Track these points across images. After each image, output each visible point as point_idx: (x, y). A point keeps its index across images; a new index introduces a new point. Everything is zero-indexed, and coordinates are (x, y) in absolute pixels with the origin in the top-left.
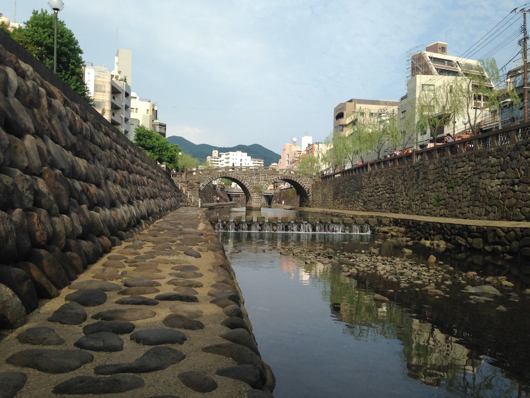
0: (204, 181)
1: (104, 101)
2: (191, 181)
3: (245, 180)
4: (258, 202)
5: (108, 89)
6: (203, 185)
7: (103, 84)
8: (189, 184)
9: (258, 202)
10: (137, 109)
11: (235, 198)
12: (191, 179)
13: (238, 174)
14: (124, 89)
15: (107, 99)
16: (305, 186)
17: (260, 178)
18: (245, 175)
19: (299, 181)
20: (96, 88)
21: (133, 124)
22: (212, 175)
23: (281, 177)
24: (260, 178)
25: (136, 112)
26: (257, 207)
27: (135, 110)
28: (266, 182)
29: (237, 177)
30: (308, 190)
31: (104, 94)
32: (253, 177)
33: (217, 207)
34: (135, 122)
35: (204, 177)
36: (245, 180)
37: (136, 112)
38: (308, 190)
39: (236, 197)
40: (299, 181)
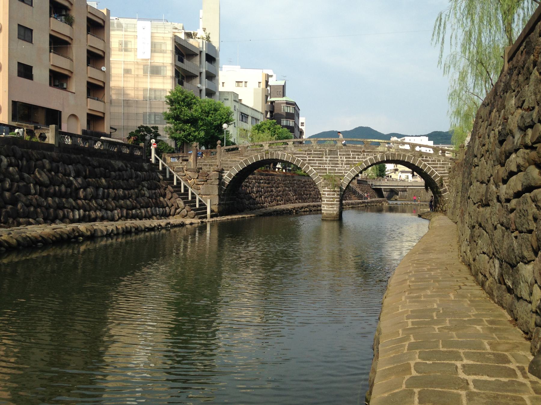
0: (231, 167)
1: (165, 65)
2: (205, 169)
3: (309, 163)
4: (332, 204)
5: (169, 47)
6: (230, 175)
7: (163, 41)
8: (202, 173)
9: (332, 204)
10: (246, 82)
11: (401, 193)
12: (206, 165)
13: (295, 154)
14: (204, 49)
15: (168, 62)
17: (339, 159)
18: (308, 154)
19: (420, 163)
20: (155, 48)
21: (228, 100)
22: (247, 156)
23: (382, 157)
24: (339, 159)
25: (246, 86)
26: (330, 214)
27: (244, 83)
28: (351, 167)
29: (294, 159)
30: (441, 180)
31: (165, 55)
32: (324, 159)
33: (303, 210)
34: (230, 96)
35: (231, 161)
36: (309, 163)
37: (246, 86)
38: (441, 180)
39: (403, 191)
40: (420, 163)
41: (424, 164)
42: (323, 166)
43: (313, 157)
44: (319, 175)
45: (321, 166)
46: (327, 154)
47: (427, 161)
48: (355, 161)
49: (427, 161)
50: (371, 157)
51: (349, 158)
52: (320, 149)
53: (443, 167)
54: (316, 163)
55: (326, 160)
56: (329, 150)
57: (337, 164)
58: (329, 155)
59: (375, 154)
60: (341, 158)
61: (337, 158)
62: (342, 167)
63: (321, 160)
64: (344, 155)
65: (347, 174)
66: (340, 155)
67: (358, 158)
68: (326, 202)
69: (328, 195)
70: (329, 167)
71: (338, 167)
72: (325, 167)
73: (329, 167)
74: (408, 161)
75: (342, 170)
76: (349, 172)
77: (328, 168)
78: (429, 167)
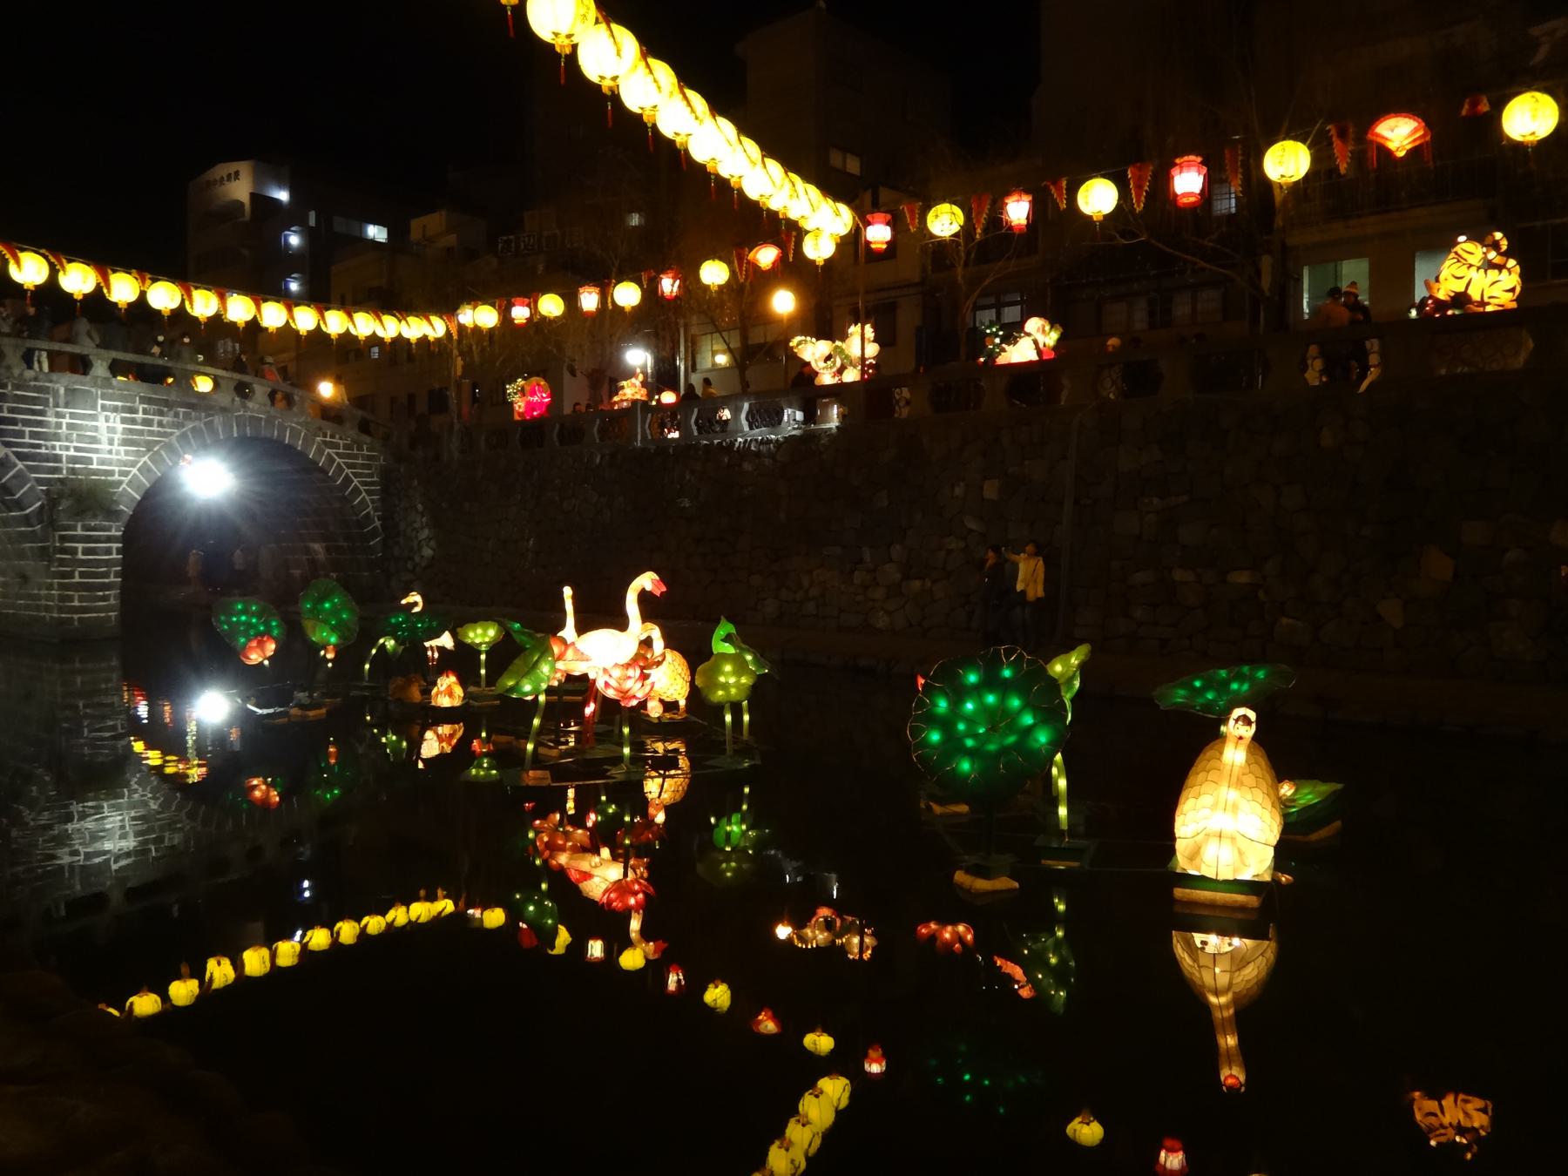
16: (348, 480)
19: (320, 452)
24: (101, 423)
41: (328, 453)
42: (49, 444)
43: (11, 410)
44: (39, 481)
45: (39, 446)
46: (62, 401)
47: (336, 446)
48: (151, 433)
49: (336, 446)
50: (196, 423)
51: (133, 421)
52: (36, 379)
53: (368, 467)
54: (21, 434)
55: (59, 426)
56: (66, 390)
57: (94, 440)
58: (67, 405)
59: (210, 415)
60: (107, 420)
61: (94, 418)
62: (110, 452)
63: (40, 424)
64: (115, 409)
65: (126, 479)
66: (104, 408)
67: (160, 424)
68: (77, 579)
69: (86, 552)
70: (67, 448)
71: (96, 451)
72: (54, 448)
73: (67, 448)
74: (292, 443)
75: (110, 464)
76: (134, 470)
77: (64, 453)
78: (339, 463)
